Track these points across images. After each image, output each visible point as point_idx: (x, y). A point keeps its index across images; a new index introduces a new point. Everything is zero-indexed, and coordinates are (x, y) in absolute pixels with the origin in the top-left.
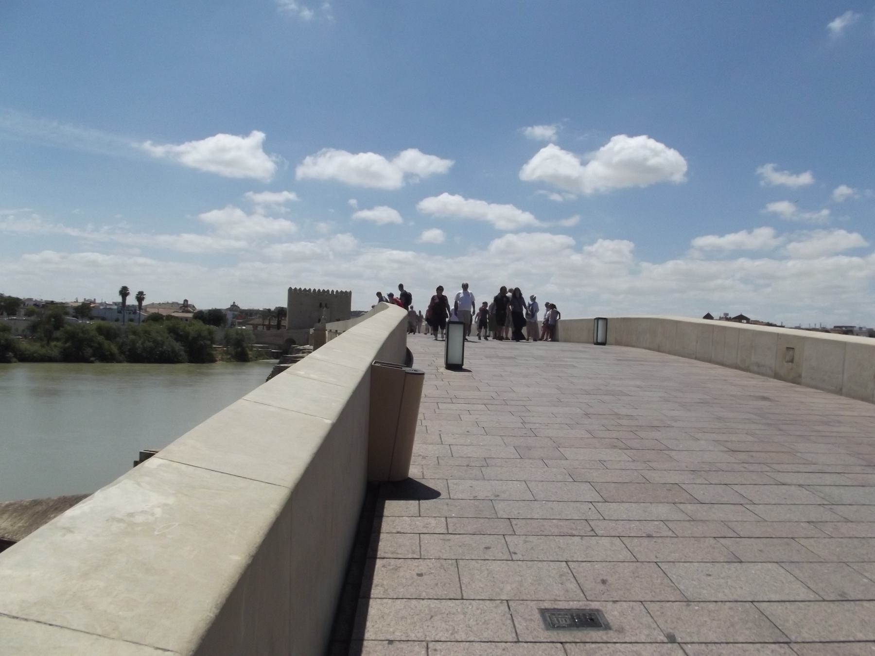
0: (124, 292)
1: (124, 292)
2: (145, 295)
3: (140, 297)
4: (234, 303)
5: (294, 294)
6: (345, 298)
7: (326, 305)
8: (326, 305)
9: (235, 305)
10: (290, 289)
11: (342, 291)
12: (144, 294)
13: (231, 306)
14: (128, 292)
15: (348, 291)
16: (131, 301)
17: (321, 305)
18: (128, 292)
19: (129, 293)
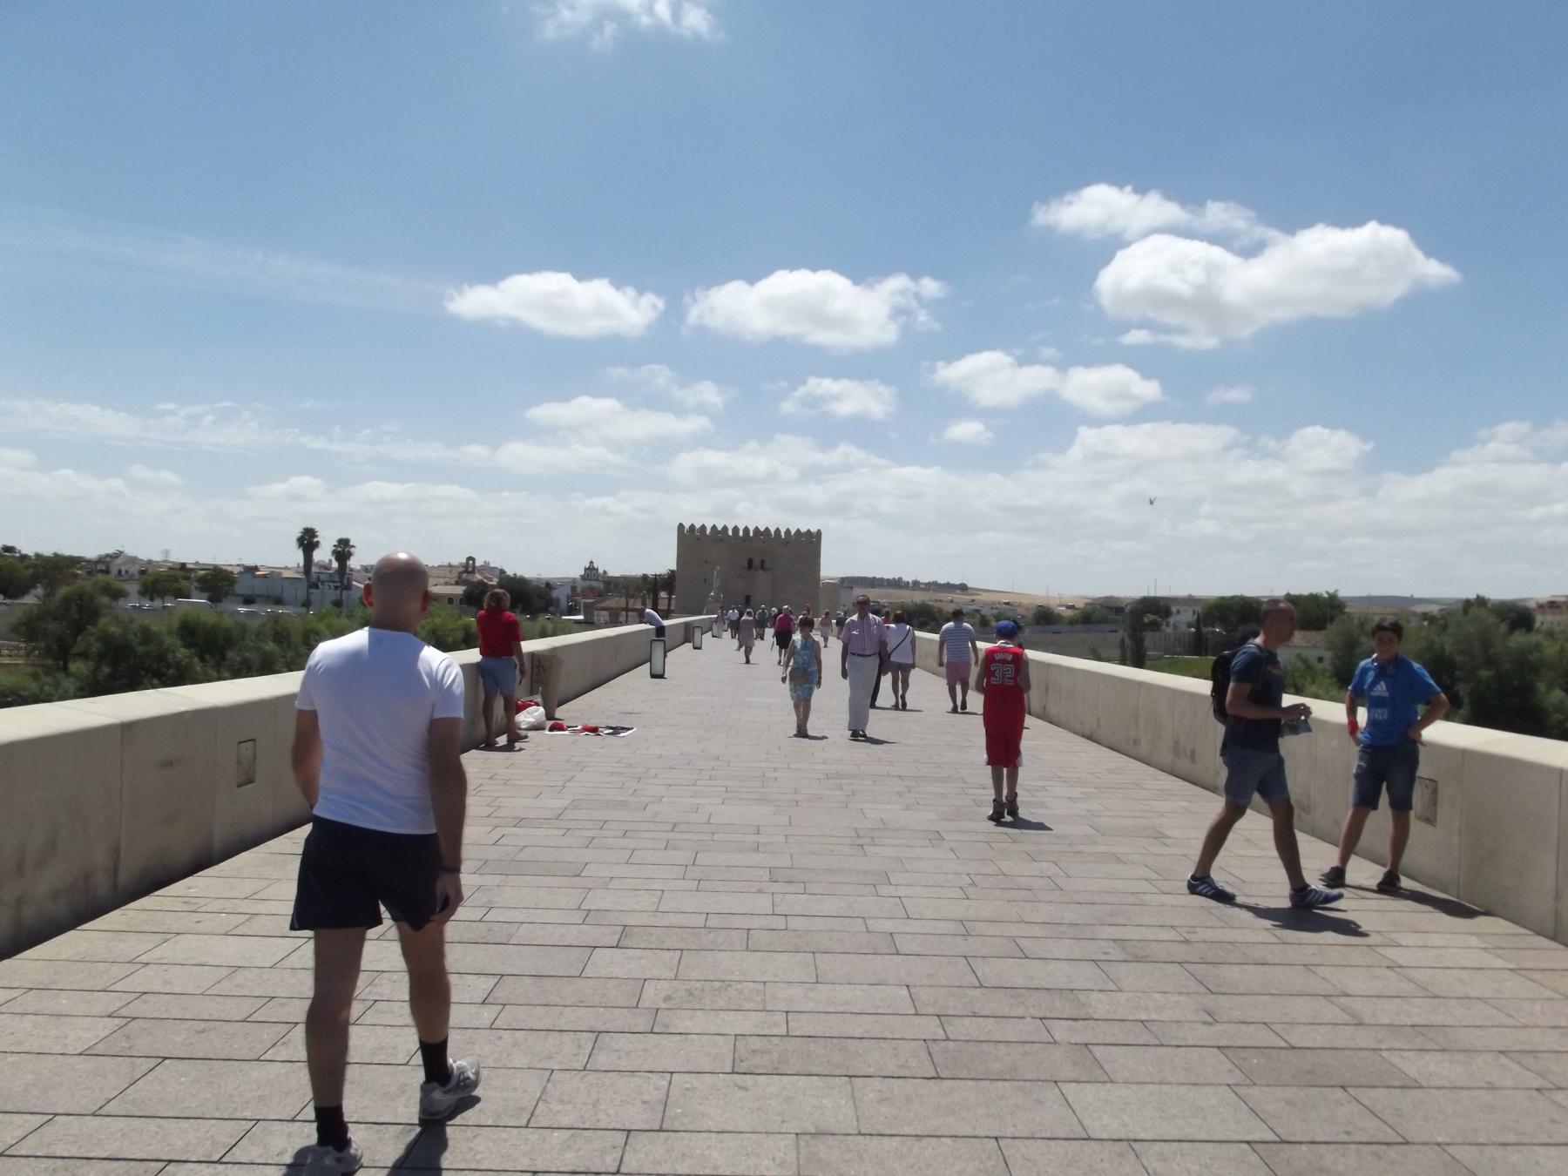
0: (308, 541)
1: (308, 541)
2: (353, 546)
3: (343, 551)
4: (591, 562)
5: (691, 540)
6: (808, 545)
7: (762, 561)
8: (762, 561)
9: (594, 568)
10: (681, 526)
11: (809, 531)
12: (351, 543)
13: (586, 569)
14: (315, 540)
15: (814, 530)
16: (323, 555)
17: (750, 563)
18: (315, 540)
19: (318, 542)
